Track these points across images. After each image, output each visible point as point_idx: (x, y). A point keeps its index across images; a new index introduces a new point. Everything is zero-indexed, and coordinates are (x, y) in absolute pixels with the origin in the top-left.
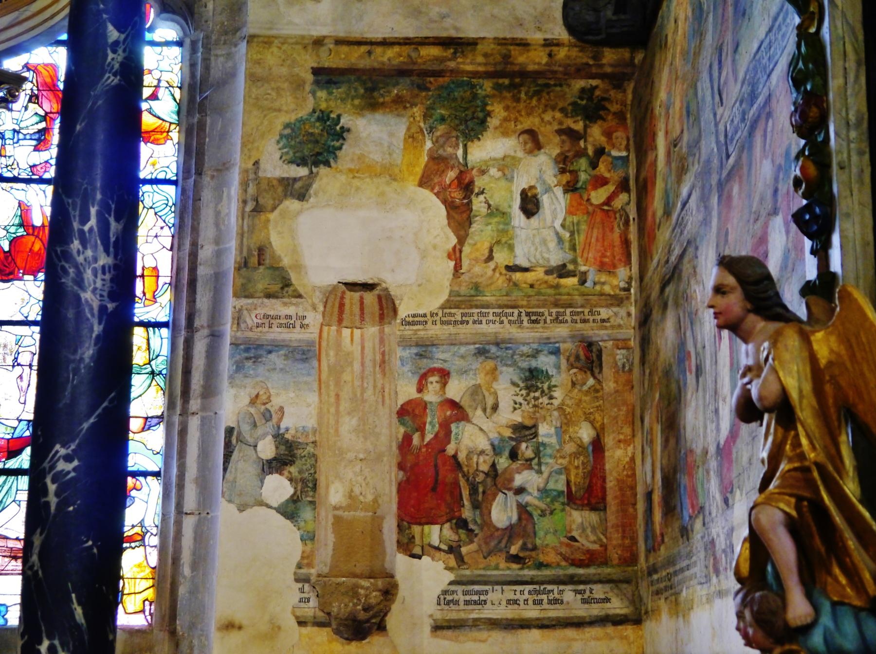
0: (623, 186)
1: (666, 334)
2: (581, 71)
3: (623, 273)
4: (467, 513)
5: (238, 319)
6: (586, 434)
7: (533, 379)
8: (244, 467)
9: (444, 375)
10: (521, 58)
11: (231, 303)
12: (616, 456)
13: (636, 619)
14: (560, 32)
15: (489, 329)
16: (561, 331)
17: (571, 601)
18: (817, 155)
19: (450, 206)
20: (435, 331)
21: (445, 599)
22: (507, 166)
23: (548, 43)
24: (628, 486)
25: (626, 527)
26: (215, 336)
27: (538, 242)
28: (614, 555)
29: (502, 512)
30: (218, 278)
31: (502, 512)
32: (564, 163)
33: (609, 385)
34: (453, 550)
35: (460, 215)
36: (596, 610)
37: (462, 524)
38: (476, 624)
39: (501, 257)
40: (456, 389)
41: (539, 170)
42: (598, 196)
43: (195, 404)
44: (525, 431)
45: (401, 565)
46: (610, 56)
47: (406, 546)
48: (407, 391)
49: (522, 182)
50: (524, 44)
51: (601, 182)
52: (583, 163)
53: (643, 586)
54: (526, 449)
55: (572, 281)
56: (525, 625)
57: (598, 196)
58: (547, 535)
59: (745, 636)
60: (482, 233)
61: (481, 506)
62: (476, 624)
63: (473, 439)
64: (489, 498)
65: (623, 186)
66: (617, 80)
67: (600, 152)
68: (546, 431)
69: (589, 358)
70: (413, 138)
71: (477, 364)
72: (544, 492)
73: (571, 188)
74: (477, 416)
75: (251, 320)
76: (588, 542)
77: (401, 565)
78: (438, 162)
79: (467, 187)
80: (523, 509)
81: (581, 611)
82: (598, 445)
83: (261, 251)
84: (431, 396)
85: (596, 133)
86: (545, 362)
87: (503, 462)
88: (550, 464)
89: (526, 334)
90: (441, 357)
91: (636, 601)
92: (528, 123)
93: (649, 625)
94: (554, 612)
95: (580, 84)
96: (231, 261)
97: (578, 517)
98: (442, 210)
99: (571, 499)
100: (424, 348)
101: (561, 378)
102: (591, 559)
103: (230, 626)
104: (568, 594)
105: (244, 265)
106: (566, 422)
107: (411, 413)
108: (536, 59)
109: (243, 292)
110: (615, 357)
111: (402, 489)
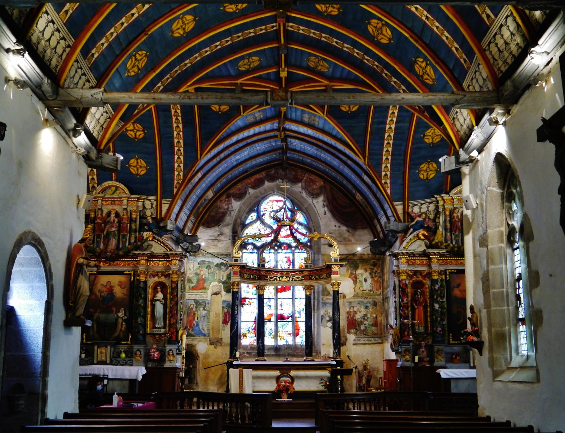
0: (380, 277)
1: (386, 305)
2: (373, 259)
3: (380, 291)
4: (357, 328)
5: (322, 299)
6: (375, 316)
7: (367, 307)
8: (324, 321)
9: (353, 307)
10: (364, 257)
11: (321, 297)
12: (379, 319)
13: (382, 343)
14: (370, 252)
15: (360, 300)
16: (371, 300)
17: (373, 341)
18: (396, 314)
19: (354, 281)
20: (352, 300)
21: (354, 340)
22: (362, 274)
23: (368, 254)
24: (381, 323)
25: (381, 329)
26: (318, 301)
27: (367, 286)
28: (379, 334)
29: (362, 328)
30: (318, 292)
31: (362, 328)
32: (370, 274)
33: (378, 308)
34: (355, 333)
35: (355, 282)
36: (376, 342)
37: (356, 329)
38: (359, 344)
39: (361, 289)
40: (355, 309)
41: (367, 275)
42: (376, 279)
43: (316, 311)
44: (366, 315)
45: (348, 335)
46: (377, 256)
47: (349, 333)
48: (348, 309)
49: (364, 277)
50: (364, 254)
51: (376, 276)
52: (373, 274)
53: (384, 339)
54: (366, 318)
55: (372, 292)
56: (366, 344)
57: (376, 279)
58: (369, 331)
59: (392, 348)
60: (358, 285)
61: (359, 326)
62: (359, 344)
63: (358, 316)
64: (360, 325)
65: (380, 277)
66: (378, 260)
67: (376, 272)
68: (369, 315)
69: (375, 304)
70: (348, 270)
71: (359, 306)
72: (369, 324)
73: (372, 277)
74: (358, 313)
75: (324, 299)
76: (375, 332)
77: (348, 335)
78: (351, 274)
79: (356, 277)
80: (366, 327)
81: (374, 342)
82: (376, 317)
83: (325, 288)
84: (351, 310)
85: (375, 269)
86: (368, 305)
87: (362, 320)
88: (369, 320)
89: (365, 300)
90: (353, 304)
91: (382, 340)
92: (365, 267)
93: (384, 344)
94: (370, 342)
95: (373, 261)
96: (321, 289)
97: (374, 328)
98: (352, 281)
99: (373, 325)
100: (350, 303)
101: (371, 307)
102: (376, 334)
103: (324, 345)
104: (372, 339)
105: (323, 291)
106: (372, 314)
107: (348, 313)
108: (366, 257)
109: (323, 295)
110: (379, 304)
111: (348, 324)
